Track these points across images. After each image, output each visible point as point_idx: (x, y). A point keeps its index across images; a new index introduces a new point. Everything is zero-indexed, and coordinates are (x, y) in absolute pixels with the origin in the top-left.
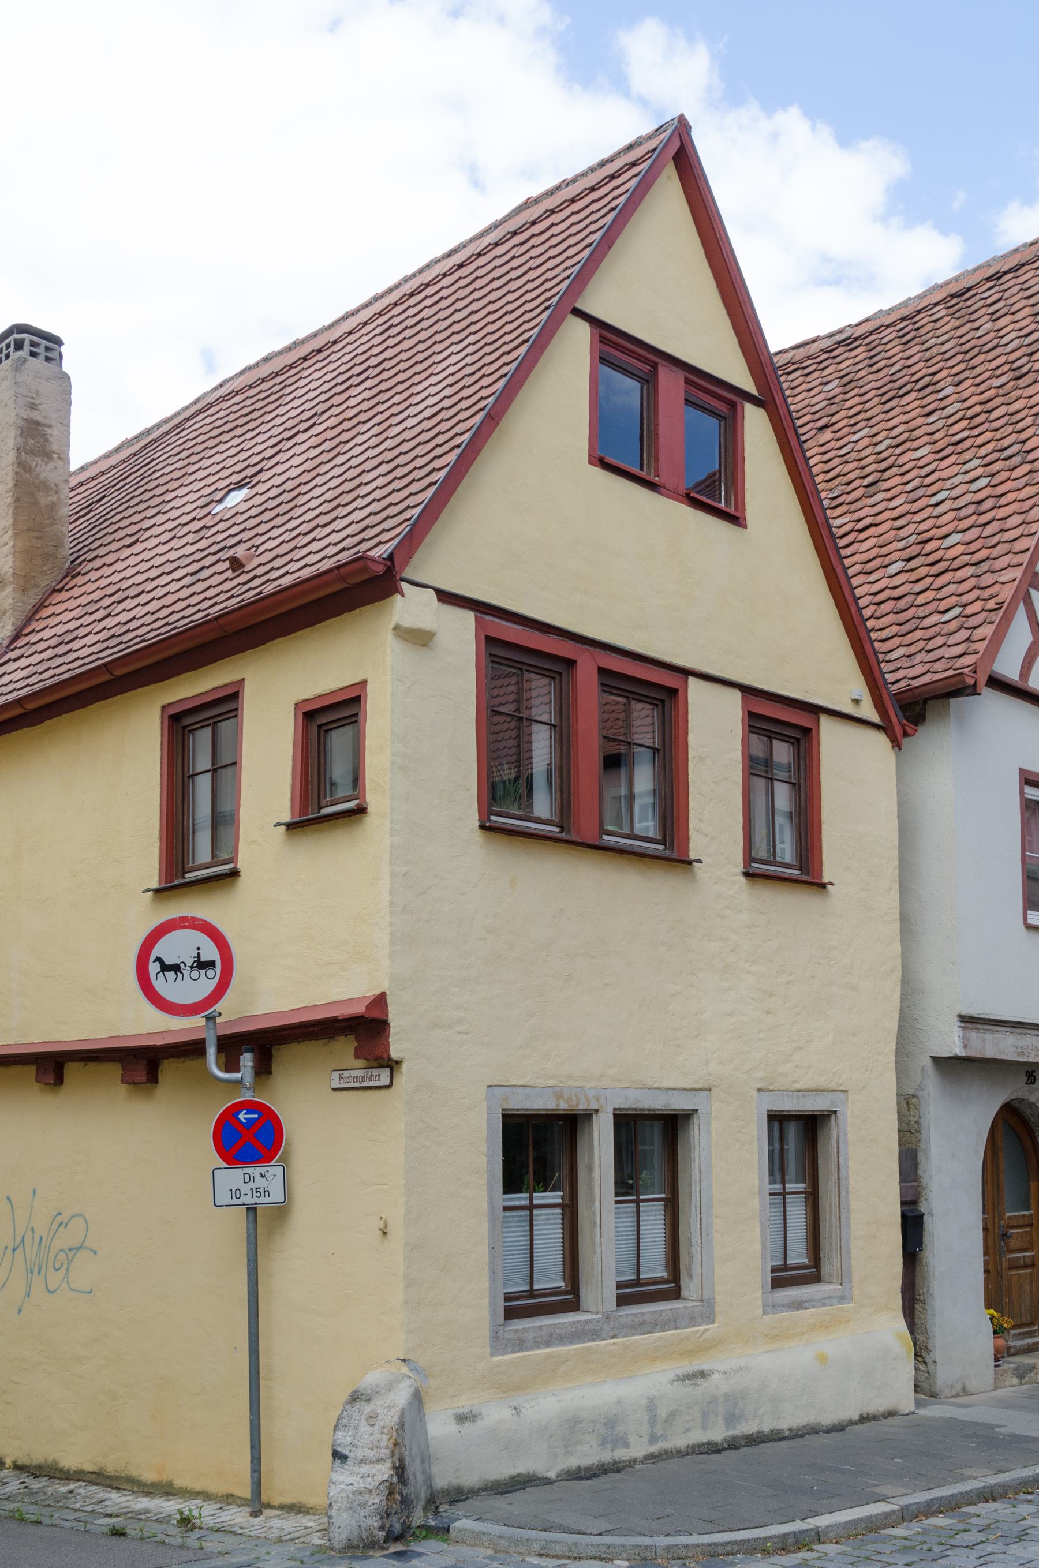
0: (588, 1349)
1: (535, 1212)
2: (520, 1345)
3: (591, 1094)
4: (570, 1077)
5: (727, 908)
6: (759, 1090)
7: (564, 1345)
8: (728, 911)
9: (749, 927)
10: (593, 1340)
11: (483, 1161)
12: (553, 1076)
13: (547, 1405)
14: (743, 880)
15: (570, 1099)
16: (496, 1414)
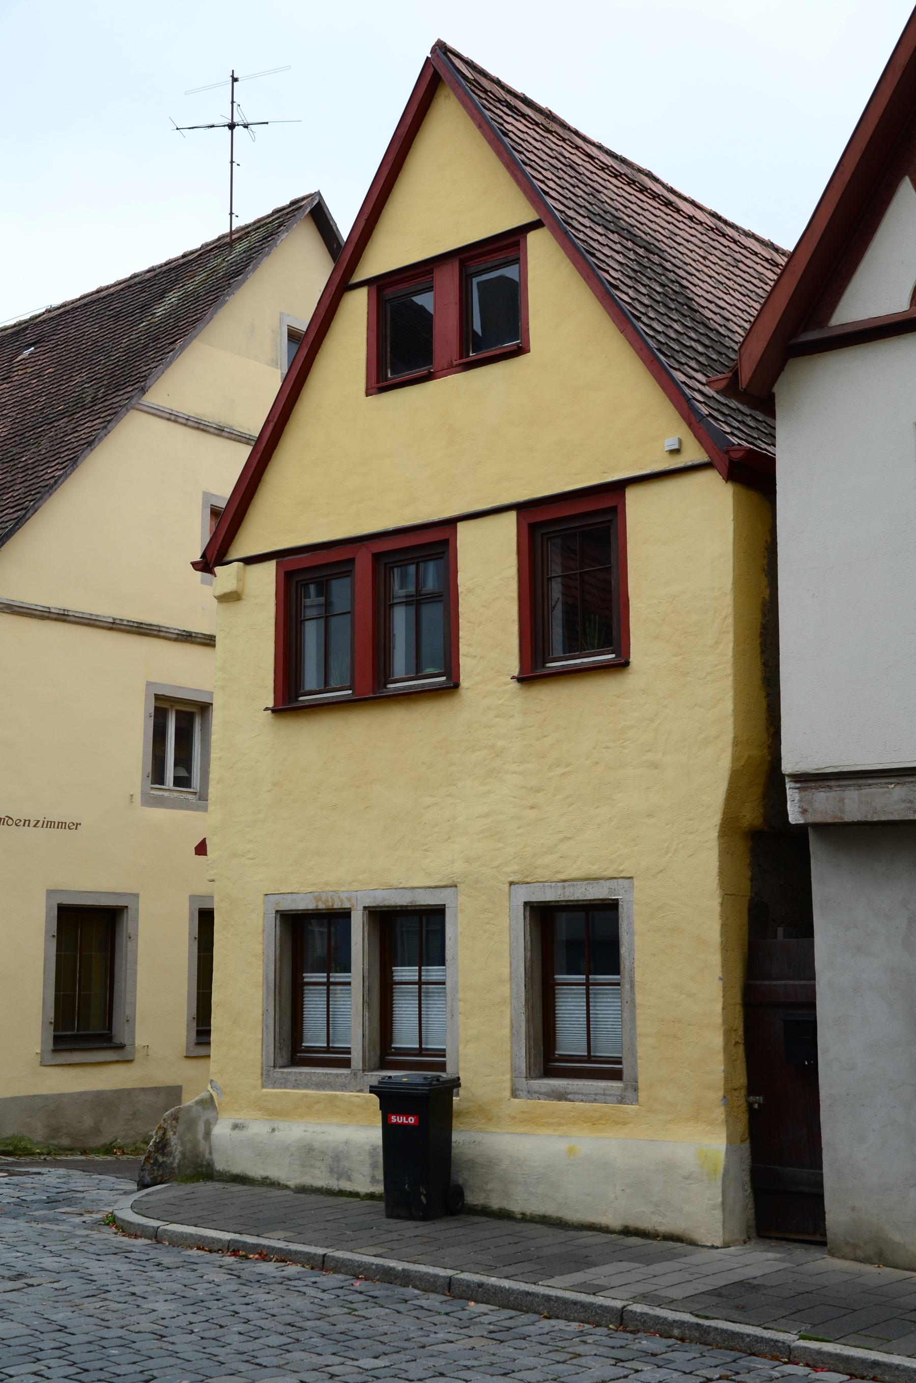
0: (336, 1096)
1: (331, 987)
2: (284, 1084)
3: (344, 896)
4: (327, 884)
5: (496, 717)
6: (511, 883)
7: (319, 1090)
8: (497, 720)
9: (520, 729)
10: (342, 1090)
11: (259, 948)
12: (314, 884)
13: (294, 1131)
14: (515, 685)
15: (327, 901)
16: (258, 1128)
